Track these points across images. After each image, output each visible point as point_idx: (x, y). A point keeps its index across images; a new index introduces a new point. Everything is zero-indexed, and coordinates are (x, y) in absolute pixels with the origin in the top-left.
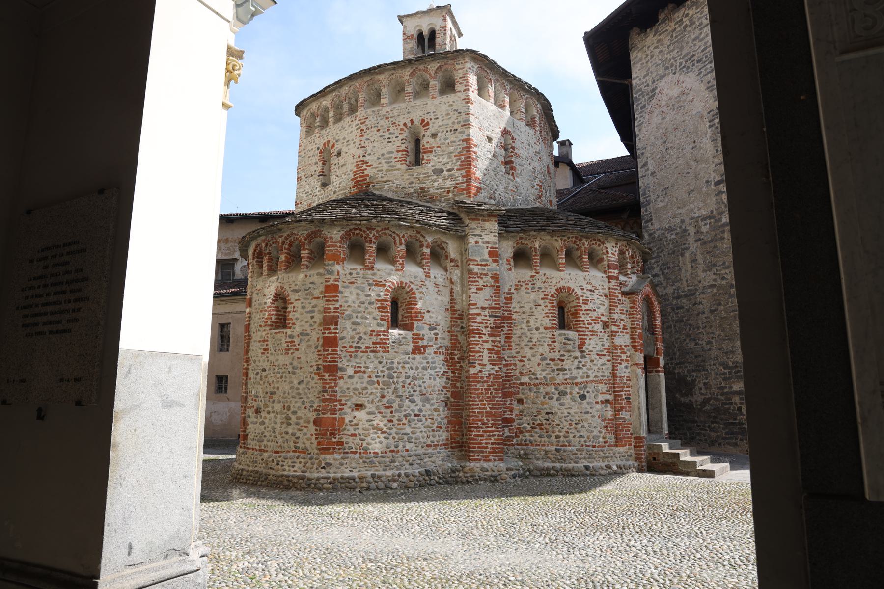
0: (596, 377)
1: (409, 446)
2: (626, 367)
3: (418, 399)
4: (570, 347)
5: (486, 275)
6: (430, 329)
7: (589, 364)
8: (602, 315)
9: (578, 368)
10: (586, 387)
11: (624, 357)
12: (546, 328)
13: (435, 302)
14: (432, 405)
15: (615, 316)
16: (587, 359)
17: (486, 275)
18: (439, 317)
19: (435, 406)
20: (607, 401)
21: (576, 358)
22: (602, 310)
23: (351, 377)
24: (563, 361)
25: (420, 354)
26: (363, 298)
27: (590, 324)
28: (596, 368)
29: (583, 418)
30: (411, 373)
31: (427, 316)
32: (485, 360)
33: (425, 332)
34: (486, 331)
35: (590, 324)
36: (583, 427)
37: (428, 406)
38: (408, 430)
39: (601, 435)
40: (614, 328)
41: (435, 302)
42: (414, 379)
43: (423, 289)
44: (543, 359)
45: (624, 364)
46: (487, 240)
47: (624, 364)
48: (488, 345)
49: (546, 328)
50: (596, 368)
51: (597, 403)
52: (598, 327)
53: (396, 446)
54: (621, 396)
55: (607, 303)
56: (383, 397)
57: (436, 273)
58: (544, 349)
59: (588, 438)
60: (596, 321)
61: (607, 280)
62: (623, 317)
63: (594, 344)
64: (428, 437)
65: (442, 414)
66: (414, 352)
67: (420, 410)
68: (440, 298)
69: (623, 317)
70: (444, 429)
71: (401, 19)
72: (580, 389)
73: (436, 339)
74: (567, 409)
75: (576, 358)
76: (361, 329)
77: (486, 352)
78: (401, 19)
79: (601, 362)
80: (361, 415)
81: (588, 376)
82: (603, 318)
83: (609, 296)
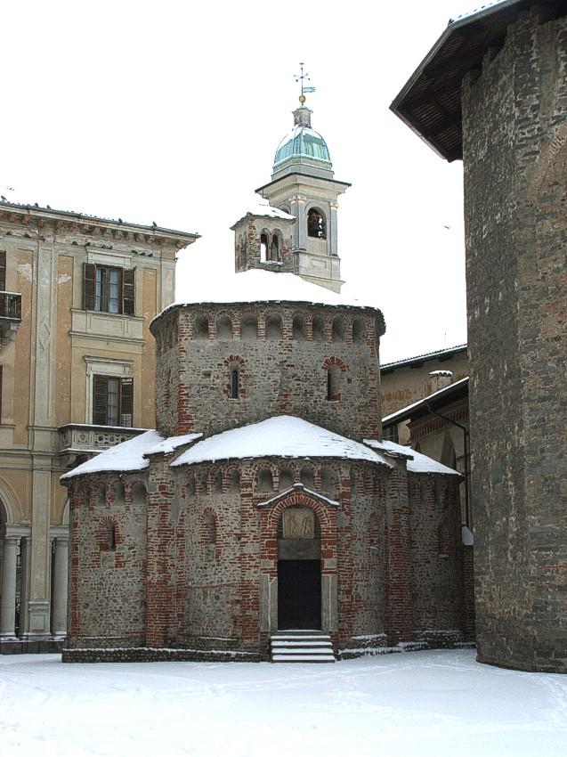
0: (228, 581)
1: (112, 632)
2: (255, 572)
3: (120, 601)
4: (210, 558)
5: (157, 505)
6: (129, 549)
7: (224, 570)
8: (235, 528)
9: (215, 574)
10: (220, 590)
11: (253, 563)
12: (199, 543)
13: (134, 528)
14: (130, 604)
15: (246, 529)
16: (223, 566)
17: (157, 505)
18: (138, 539)
19: (133, 604)
20: (238, 601)
21: (214, 566)
22: (236, 525)
23: (83, 585)
24: (206, 568)
25: (121, 566)
26: (89, 531)
27: (224, 537)
28: (228, 574)
29: (216, 617)
30: (114, 581)
31: (127, 539)
32: (155, 571)
33: (125, 551)
34: (157, 548)
35: (224, 537)
36: (217, 622)
37: (126, 604)
38: (112, 622)
39: (230, 629)
40: (245, 540)
41: (134, 528)
42: (116, 585)
43: (124, 520)
44: (197, 568)
45: (253, 570)
46: (159, 477)
47: (253, 570)
48: (156, 559)
49: (199, 543)
50: (228, 574)
51: (228, 602)
52: (230, 540)
53: (105, 632)
54: (248, 596)
55: (239, 518)
56: (98, 598)
57: (137, 508)
58: (197, 559)
59: (220, 631)
60: (229, 535)
61: (240, 498)
62: (254, 528)
63: (228, 554)
64: (127, 626)
65: (139, 610)
66: (116, 567)
67: (121, 608)
68: (139, 525)
69: (254, 528)
70: (140, 621)
71: (232, 228)
72: (216, 591)
73: (134, 555)
74: (207, 606)
75: (214, 566)
76: (88, 552)
77: (156, 564)
78: (232, 228)
79: (233, 568)
80: (87, 611)
81: (222, 581)
82: (236, 531)
83: (241, 512)
